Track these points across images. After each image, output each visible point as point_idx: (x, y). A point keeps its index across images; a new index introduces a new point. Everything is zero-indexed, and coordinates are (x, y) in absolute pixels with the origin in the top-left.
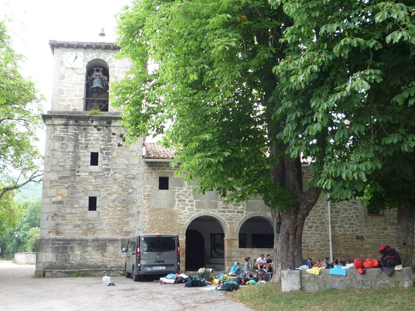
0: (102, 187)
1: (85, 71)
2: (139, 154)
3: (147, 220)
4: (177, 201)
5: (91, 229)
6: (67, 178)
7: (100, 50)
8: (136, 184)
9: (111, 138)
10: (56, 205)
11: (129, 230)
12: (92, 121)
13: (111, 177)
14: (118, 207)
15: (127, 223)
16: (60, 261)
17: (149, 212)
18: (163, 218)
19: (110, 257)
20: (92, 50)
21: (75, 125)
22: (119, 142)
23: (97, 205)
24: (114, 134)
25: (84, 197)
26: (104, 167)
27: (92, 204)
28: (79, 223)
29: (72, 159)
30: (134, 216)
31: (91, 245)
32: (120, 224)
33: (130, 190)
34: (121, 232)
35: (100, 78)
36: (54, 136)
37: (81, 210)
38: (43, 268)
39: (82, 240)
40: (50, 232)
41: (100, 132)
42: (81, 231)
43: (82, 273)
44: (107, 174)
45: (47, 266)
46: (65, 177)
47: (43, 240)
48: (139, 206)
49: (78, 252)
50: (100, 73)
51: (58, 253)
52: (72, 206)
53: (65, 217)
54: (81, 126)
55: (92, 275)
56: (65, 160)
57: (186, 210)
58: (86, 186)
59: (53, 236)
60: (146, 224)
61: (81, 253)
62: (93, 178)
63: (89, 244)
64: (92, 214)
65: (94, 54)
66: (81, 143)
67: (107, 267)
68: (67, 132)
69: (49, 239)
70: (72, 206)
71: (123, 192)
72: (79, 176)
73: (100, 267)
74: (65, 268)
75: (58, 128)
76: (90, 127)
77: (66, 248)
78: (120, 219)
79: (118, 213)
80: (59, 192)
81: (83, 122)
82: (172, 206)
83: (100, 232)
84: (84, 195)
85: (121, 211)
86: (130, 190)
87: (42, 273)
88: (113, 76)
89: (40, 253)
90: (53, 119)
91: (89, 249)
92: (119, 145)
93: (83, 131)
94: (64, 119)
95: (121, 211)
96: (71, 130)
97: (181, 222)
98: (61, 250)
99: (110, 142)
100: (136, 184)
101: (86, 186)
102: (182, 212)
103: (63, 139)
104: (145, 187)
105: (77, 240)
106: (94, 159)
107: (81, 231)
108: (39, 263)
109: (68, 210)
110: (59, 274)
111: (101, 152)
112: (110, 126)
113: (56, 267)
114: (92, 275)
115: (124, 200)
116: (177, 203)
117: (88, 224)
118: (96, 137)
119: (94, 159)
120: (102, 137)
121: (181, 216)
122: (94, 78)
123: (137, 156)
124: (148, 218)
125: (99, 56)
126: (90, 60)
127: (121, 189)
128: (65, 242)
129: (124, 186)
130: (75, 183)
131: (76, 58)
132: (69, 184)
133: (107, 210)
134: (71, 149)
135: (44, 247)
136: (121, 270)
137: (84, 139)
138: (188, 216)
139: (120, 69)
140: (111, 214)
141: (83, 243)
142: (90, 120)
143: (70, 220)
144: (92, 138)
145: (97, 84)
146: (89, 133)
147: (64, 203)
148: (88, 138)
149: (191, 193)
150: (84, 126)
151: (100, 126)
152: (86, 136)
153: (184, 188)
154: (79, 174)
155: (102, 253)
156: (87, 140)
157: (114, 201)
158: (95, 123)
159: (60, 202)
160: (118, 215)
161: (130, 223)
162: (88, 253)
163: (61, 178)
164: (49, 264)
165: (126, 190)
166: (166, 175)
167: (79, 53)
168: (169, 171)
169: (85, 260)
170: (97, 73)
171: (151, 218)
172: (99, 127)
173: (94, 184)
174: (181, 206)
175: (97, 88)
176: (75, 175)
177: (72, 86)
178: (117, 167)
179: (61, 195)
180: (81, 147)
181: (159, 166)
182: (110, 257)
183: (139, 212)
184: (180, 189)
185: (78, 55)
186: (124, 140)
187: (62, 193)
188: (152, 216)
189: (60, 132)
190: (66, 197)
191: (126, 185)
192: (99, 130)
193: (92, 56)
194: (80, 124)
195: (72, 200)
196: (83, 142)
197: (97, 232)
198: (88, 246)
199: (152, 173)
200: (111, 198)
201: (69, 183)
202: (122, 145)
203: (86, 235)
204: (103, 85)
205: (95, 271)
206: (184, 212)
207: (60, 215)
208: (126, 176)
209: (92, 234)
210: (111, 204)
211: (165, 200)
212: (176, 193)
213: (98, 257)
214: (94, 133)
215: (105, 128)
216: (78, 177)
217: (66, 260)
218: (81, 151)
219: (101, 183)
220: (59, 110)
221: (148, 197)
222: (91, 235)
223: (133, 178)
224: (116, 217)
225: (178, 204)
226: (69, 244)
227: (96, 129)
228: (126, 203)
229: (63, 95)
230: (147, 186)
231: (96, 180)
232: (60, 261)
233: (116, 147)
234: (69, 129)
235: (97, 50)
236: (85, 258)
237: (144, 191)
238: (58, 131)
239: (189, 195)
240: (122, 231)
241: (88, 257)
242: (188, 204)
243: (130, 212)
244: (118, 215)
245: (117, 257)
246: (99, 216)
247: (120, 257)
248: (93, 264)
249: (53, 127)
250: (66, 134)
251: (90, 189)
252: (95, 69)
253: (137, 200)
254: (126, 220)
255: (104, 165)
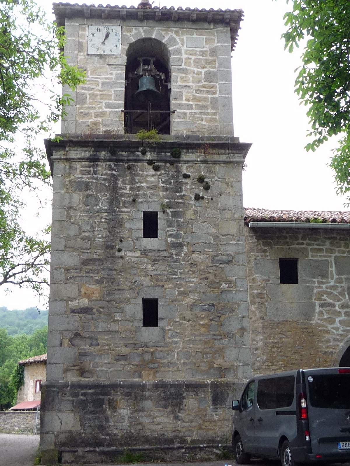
0: (169, 280)
1: (124, 60)
2: (237, 215)
3: (261, 344)
4: (318, 307)
5: (150, 363)
6: (97, 263)
7: (151, 23)
8: (234, 273)
9: (181, 183)
10: (77, 316)
11: (226, 365)
12: (144, 153)
13: (184, 260)
14: (202, 319)
15: (221, 351)
16: (89, 430)
17: (263, 328)
18: (291, 340)
19: (191, 421)
20: (137, 23)
21: (110, 160)
22: (197, 191)
23: (160, 315)
24: (186, 176)
25: (133, 301)
26: (169, 240)
27: (150, 313)
28: (126, 351)
29: (106, 226)
30: (233, 336)
31: (149, 396)
32: (206, 353)
33: (224, 286)
34: (210, 369)
35: (152, 76)
36: (70, 181)
37: (128, 325)
38: (55, 444)
39: (132, 386)
40: (66, 371)
41: (158, 173)
42: (129, 368)
43: (137, 454)
44: (177, 255)
45: (63, 440)
46: (95, 260)
47: (54, 386)
48: (243, 317)
49: (125, 411)
50: (151, 67)
51: (85, 413)
52: (110, 316)
53: (97, 340)
54: (122, 161)
55: (158, 458)
56: (92, 226)
57: (337, 324)
58: (137, 278)
59: (72, 378)
60: (259, 352)
61: (132, 413)
62: (150, 261)
63: (147, 394)
64: (150, 334)
65: (141, 29)
66: (123, 195)
67: (185, 441)
68: (95, 173)
69: (66, 385)
70: (110, 316)
71: (209, 290)
72: (121, 257)
73: (171, 441)
74: (100, 444)
75: (78, 166)
76: (140, 164)
77: (102, 402)
78: (206, 343)
79: (203, 330)
80: (83, 291)
81: (125, 154)
82: (308, 314)
83: (167, 369)
84: (133, 295)
85: (207, 326)
86: (224, 286)
87: (57, 454)
88: (179, 69)
89: (47, 413)
90: (67, 149)
91: (148, 404)
92: (198, 198)
93: (127, 172)
94: (89, 149)
95: (207, 326)
96: (103, 170)
97: (327, 347)
98: (90, 407)
99: (180, 192)
100: (234, 273)
101: (137, 278)
102: (330, 327)
103: (87, 186)
104: (253, 279)
105: (123, 387)
106: (150, 226)
107: (129, 368)
108: (47, 433)
109: (102, 326)
110: (90, 456)
111: (164, 212)
112: (179, 162)
113: (82, 443)
114: (158, 458)
115: (213, 305)
116: (318, 309)
117: (144, 353)
118: (152, 182)
119: (150, 226)
120: (163, 183)
121: (327, 336)
122: (142, 76)
123: (233, 219)
124: (262, 340)
125: (151, 32)
126: (133, 40)
127: (204, 282)
128: (98, 391)
129: (211, 277)
130: (115, 272)
131: (107, 36)
132: (103, 273)
133: (180, 324)
134: (103, 205)
135: (57, 401)
136: (217, 448)
137: (128, 187)
138: (341, 335)
139: (190, 57)
140: (188, 332)
141: (135, 393)
142: (140, 149)
143: (107, 345)
144: (144, 185)
145: (146, 84)
146: (138, 175)
147: (95, 311)
148: (137, 185)
149: (343, 290)
150: (129, 161)
151: (158, 161)
152: (133, 181)
153: (330, 280)
154: (122, 253)
155: (174, 412)
156: (135, 188)
157: (192, 307)
158: (149, 156)
159: (86, 310)
160: (201, 335)
161: (227, 351)
162: (145, 413)
163: (85, 262)
164: (67, 435)
165: (215, 285)
166: (294, 255)
167: (111, 28)
168: (297, 246)
169: (140, 427)
170: (146, 67)
171: (268, 340)
172: (157, 164)
173: (152, 273)
174: (325, 317)
175: (148, 91)
176: (113, 257)
177: (100, 88)
178: (194, 241)
179: (87, 296)
180: (124, 203)
181: (279, 238)
182: (191, 421)
183: (243, 329)
184: (323, 283)
185: (110, 31)
186: (207, 188)
187: (88, 292)
188: (269, 336)
189: (82, 172)
190: (96, 300)
191: (216, 276)
192: (156, 169)
193: (137, 32)
194: (122, 158)
195: (109, 305)
196: (127, 191)
197: (162, 369)
198: (145, 399)
199: (265, 251)
200: (187, 300)
201: (103, 272)
202: (203, 198)
203: (141, 376)
204: (157, 87)
205: (164, 449)
206: (333, 328)
207: (86, 335)
208: (213, 257)
209: (151, 373)
210: (188, 314)
211: (294, 305)
212: (316, 291)
213: (165, 420)
214: (147, 176)
215: (168, 165)
216: (121, 261)
217: (102, 428)
218: (124, 209)
219: (166, 273)
220: (79, 132)
221: (261, 299)
222: (149, 375)
223: (229, 262)
224: (198, 338)
225: (321, 313)
226: (106, 394)
227: (151, 167)
228: (217, 311)
229: (85, 106)
230: (256, 276)
231: (156, 266)
232: (89, 430)
233: (192, 202)
234: (99, 168)
235: (145, 23)
236: (140, 424)
237: (251, 286)
238: (78, 171)
239: (340, 293)
240: (211, 367)
241: (146, 420)
242: (340, 312)
243: (226, 328)
244: (201, 335)
245: (204, 421)
246: (164, 336)
247: (211, 421)
248: (156, 434)
249: (67, 164)
250: (93, 178)
251: (145, 284)
252: (141, 59)
253: (239, 305)
254: (218, 344)
255: (171, 236)
